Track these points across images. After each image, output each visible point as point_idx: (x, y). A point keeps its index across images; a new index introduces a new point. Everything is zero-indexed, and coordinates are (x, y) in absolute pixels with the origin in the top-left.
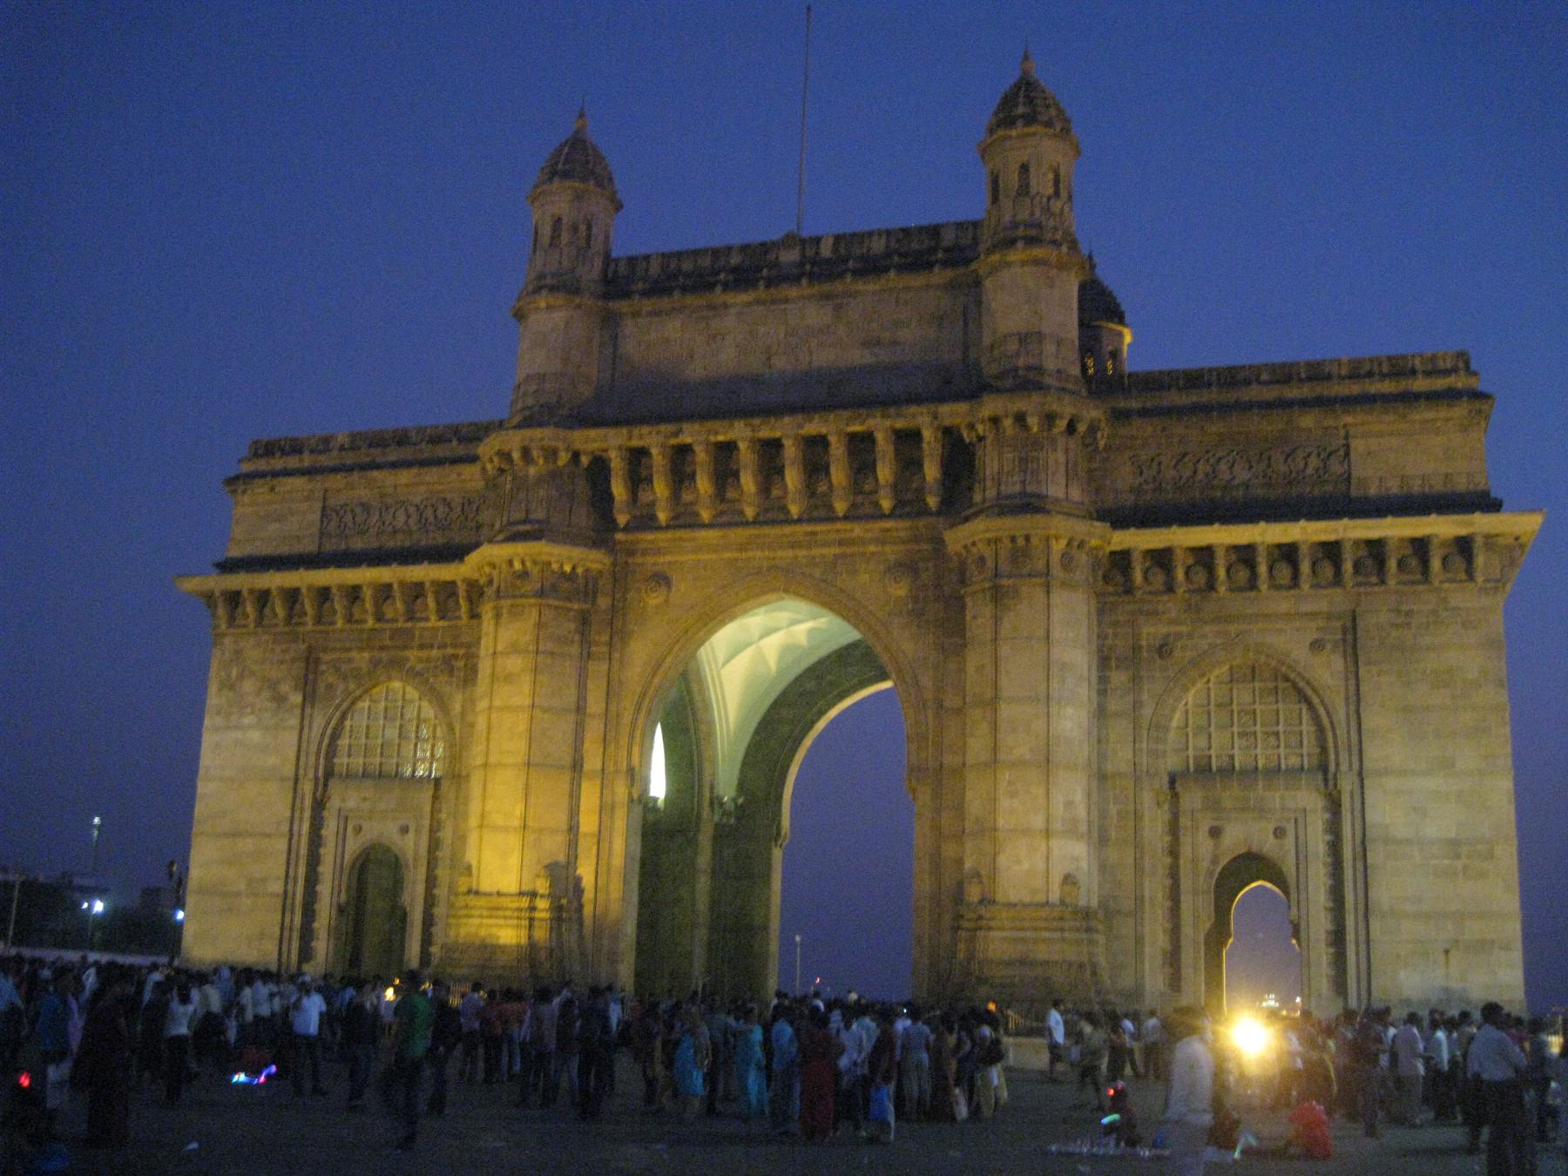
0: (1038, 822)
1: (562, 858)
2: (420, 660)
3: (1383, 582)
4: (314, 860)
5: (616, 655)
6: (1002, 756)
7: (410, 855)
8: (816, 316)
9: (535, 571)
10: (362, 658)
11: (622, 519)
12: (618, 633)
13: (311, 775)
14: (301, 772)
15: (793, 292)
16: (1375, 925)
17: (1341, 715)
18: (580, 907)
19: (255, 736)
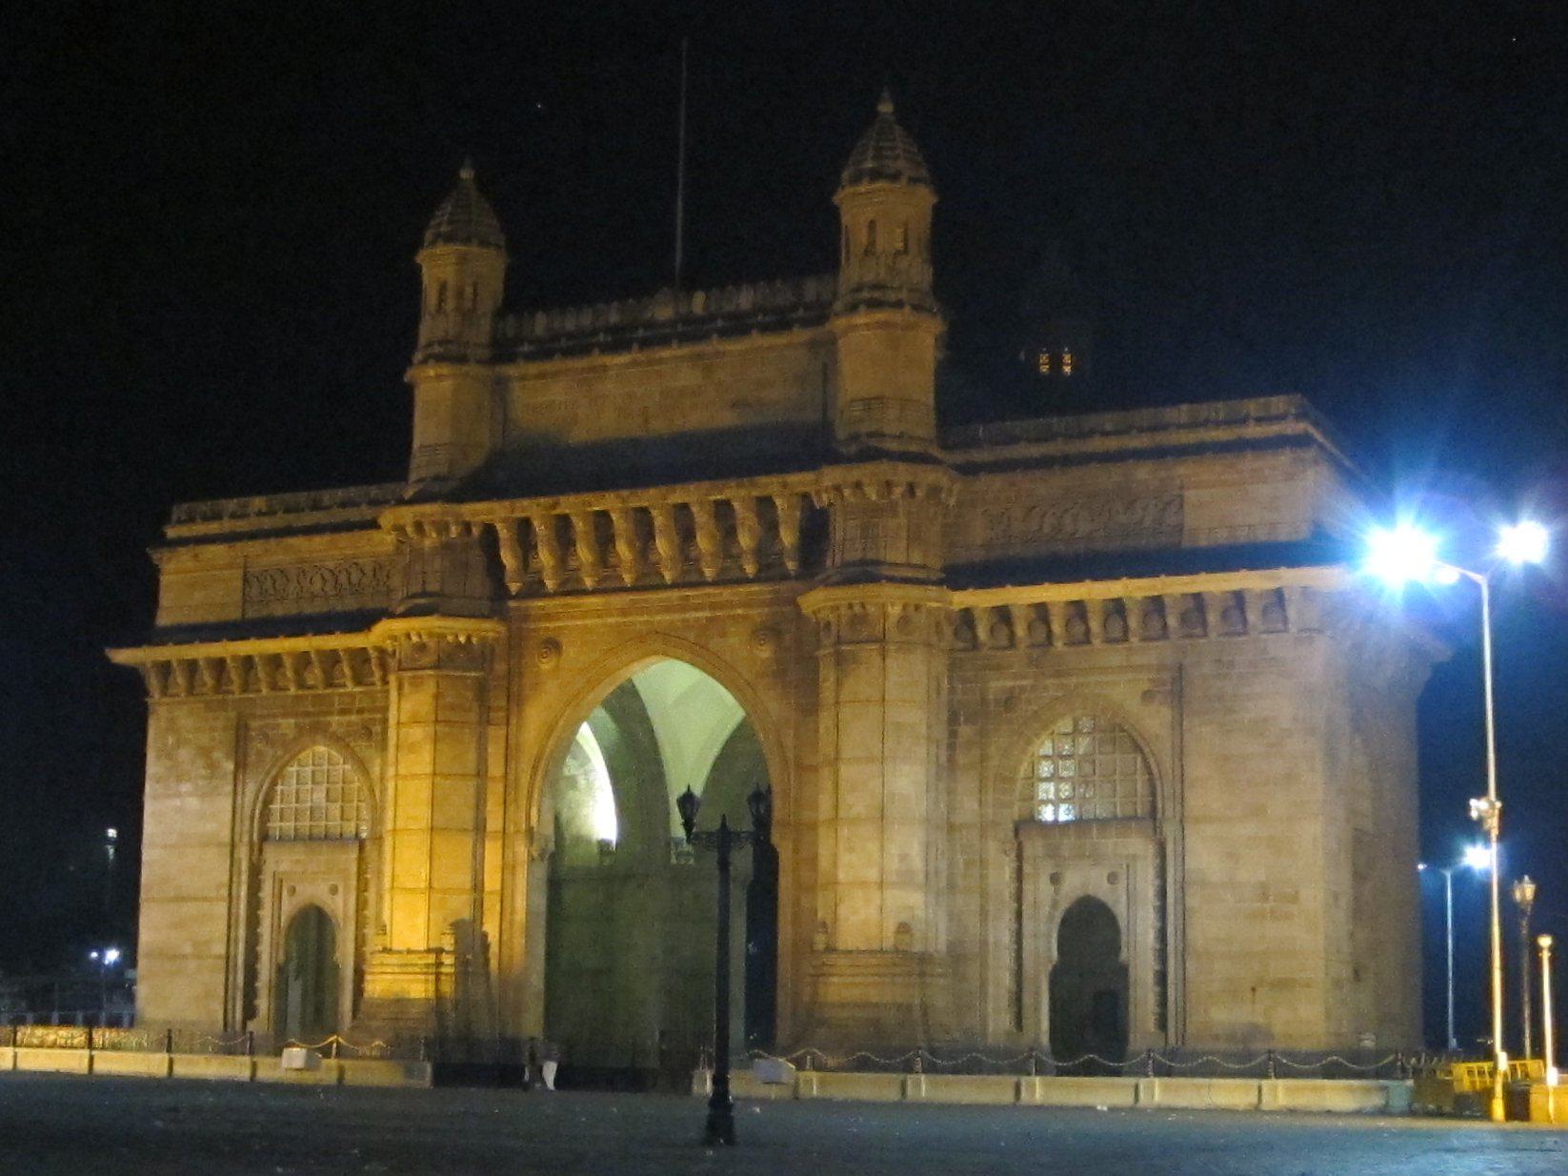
0: (873, 874)
1: (466, 914)
2: (340, 724)
3: (1205, 635)
4: (253, 922)
5: (513, 721)
6: (842, 814)
7: (340, 914)
8: (688, 377)
9: (432, 644)
10: (287, 725)
11: (514, 587)
12: (515, 700)
13: (246, 839)
14: (237, 838)
15: (665, 353)
16: (1191, 966)
17: (1167, 764)
18: (487, 961)
19: (193, 803)
